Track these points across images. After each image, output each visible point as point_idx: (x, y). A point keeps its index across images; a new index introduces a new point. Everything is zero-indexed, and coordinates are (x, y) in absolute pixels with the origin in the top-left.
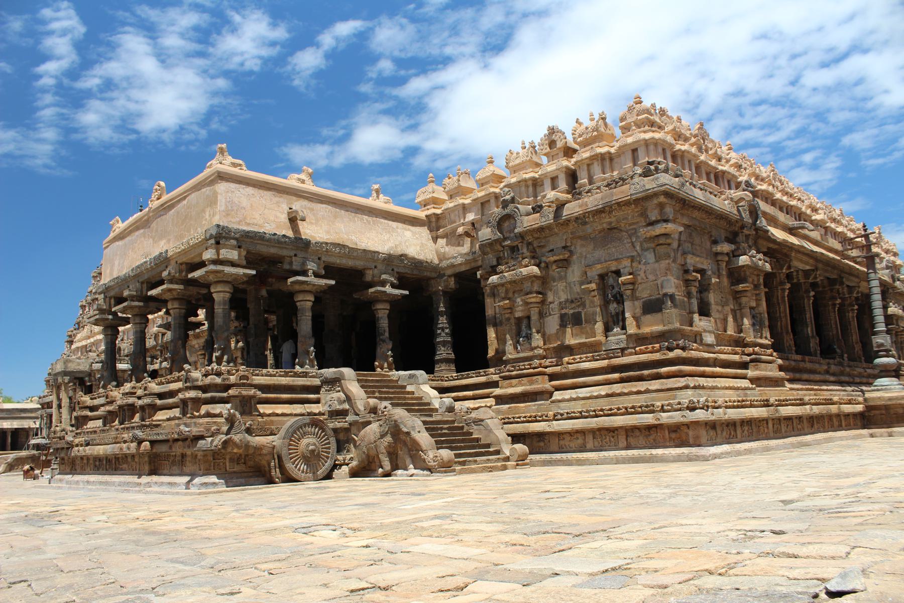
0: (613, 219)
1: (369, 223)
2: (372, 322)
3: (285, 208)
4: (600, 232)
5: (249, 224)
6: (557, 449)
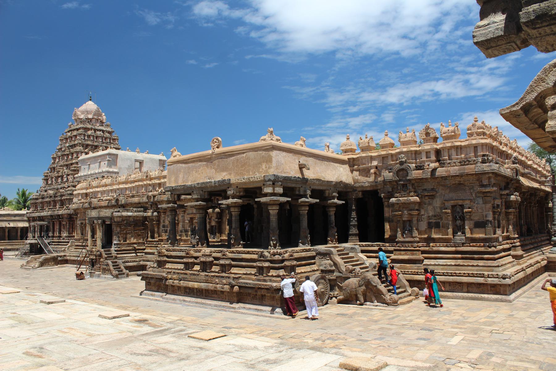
0: (462, 180)
4: (453, 184)
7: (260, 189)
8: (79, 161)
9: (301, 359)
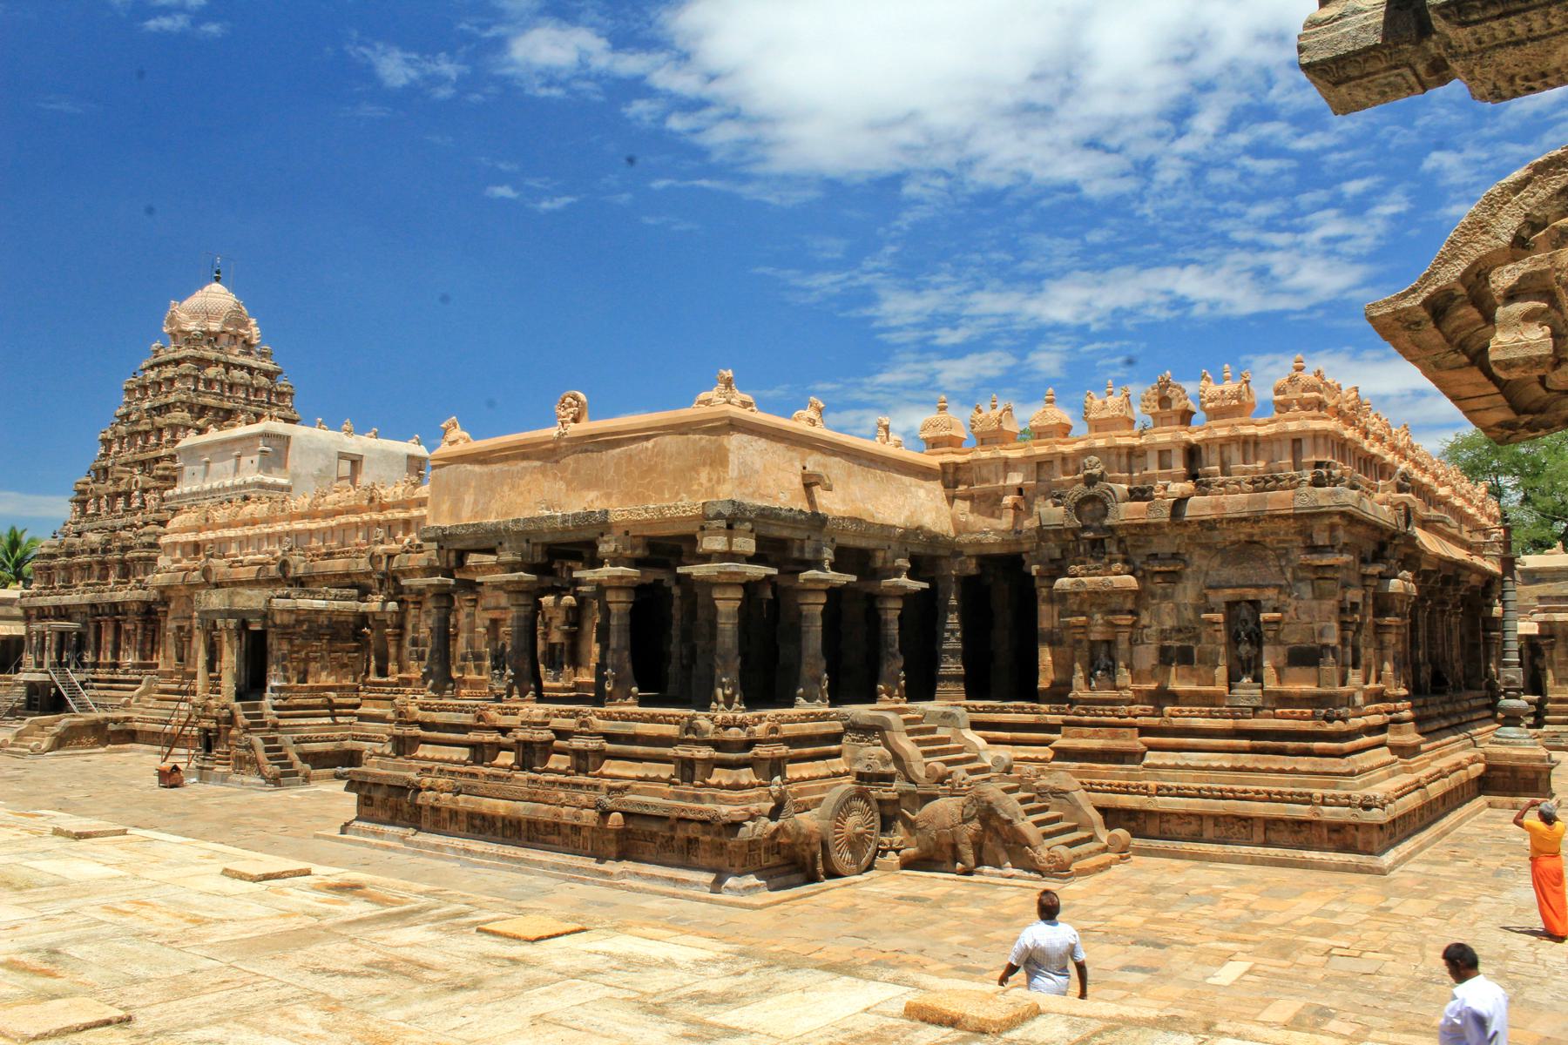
0: (1256, 531)
4: (1233, 543)
6: (1156, 833)
7: (692, 540)
8: (178, 451)
9: (798, 994)
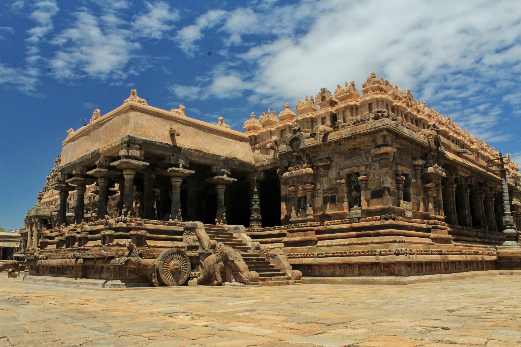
0: (356, 143)
1: (216, 139)
2: (215, 196)
3: (168, 128)
4: (348, 150)
5: (147, 136)
